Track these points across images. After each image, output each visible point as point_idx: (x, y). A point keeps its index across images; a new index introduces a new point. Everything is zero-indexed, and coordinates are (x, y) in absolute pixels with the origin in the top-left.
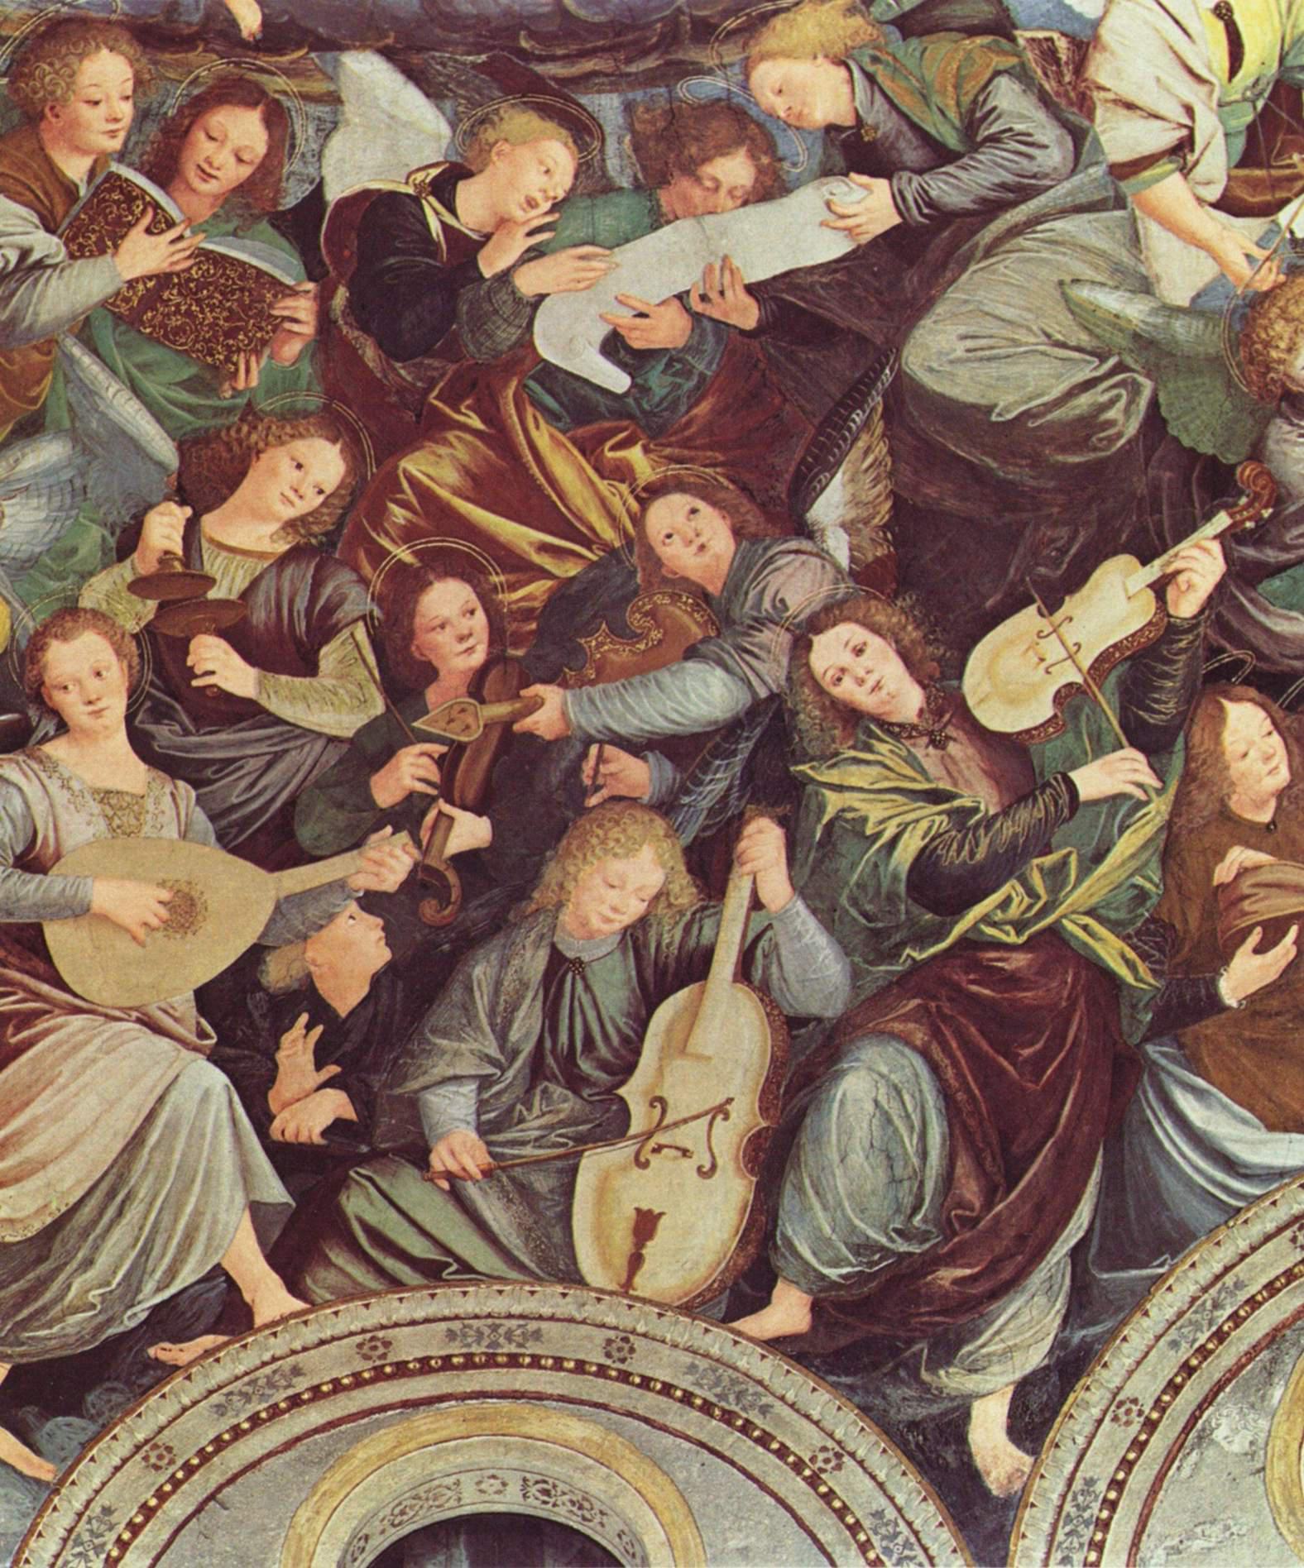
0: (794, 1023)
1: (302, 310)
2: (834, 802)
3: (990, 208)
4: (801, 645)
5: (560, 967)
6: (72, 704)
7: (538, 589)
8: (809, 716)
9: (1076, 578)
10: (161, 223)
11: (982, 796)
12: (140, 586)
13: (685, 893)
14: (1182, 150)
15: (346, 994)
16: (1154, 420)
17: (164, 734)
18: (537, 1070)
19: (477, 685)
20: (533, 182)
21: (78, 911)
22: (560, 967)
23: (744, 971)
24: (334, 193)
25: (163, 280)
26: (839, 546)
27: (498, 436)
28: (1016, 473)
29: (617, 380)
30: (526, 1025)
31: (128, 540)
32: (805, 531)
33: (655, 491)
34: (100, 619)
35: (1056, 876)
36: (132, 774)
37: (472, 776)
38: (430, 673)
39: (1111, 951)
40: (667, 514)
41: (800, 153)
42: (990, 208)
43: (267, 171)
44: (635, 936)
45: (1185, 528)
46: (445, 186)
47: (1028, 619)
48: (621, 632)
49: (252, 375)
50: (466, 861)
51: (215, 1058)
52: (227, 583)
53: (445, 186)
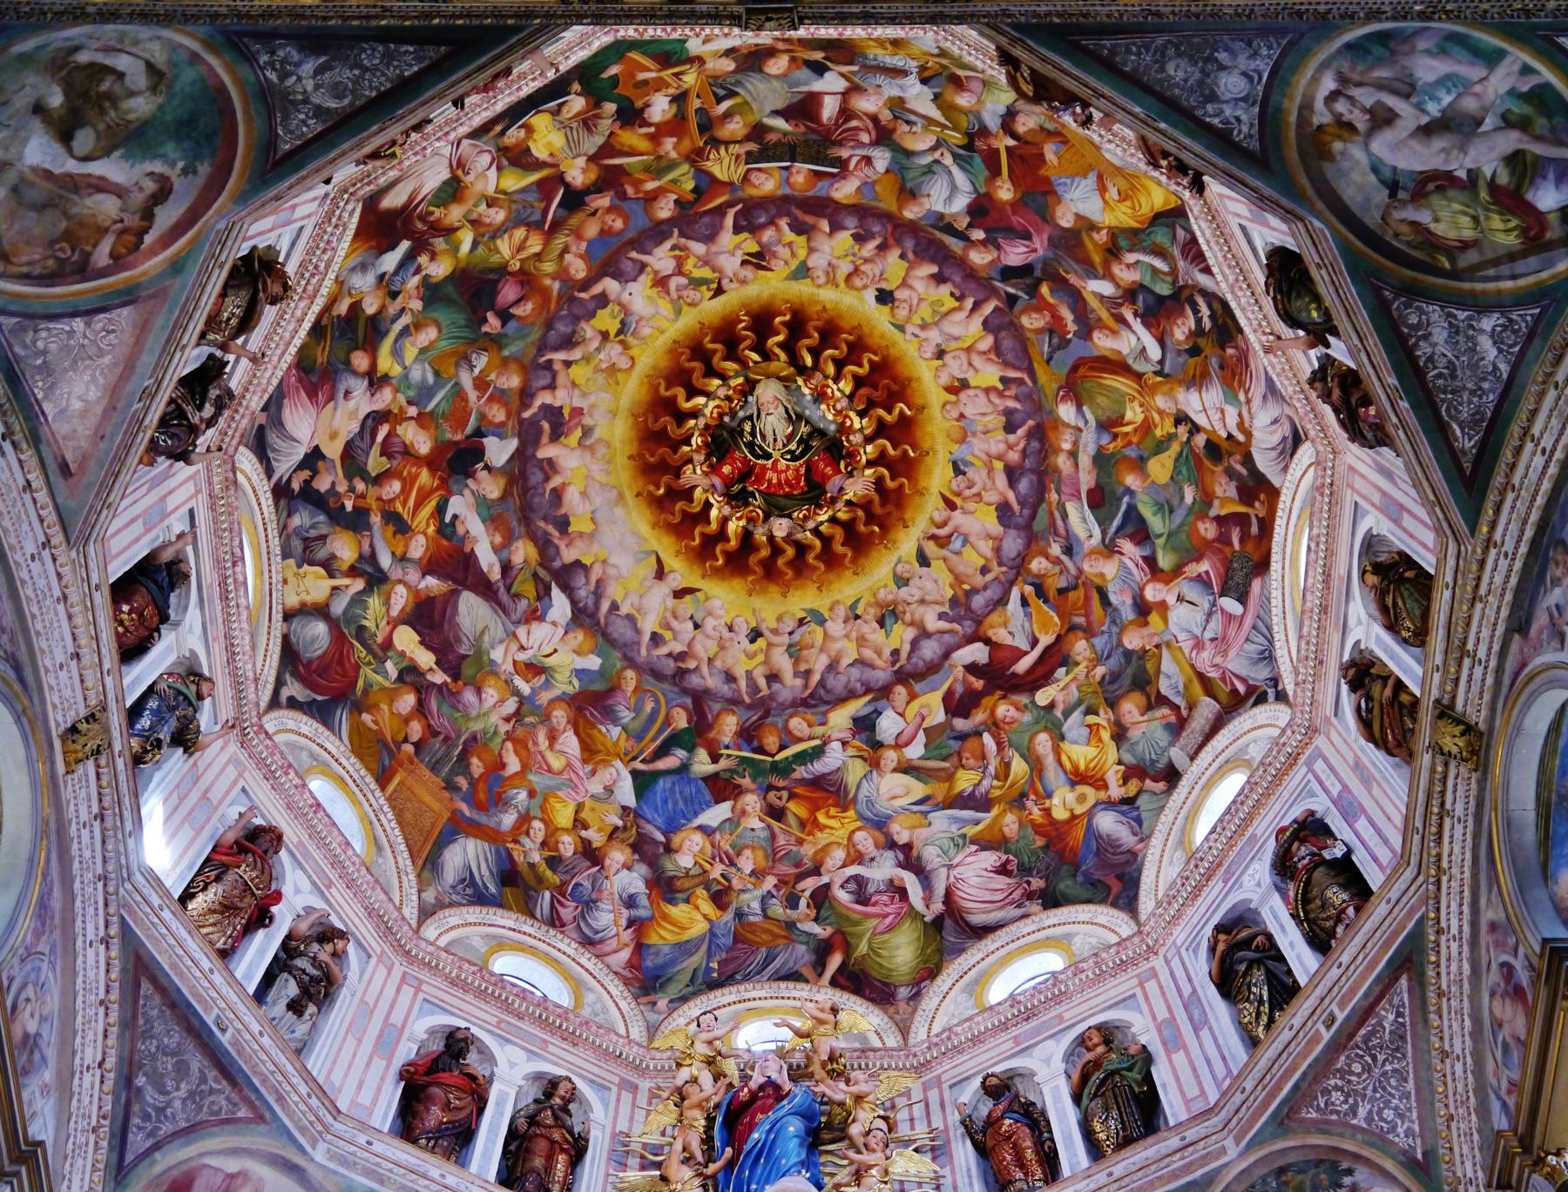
0: (327, 605)
1: (458, 437)
2: (370, 600)
3: (499, 604)
4: (400, 581)
5: (323, 538)
6: (378, 396)
7: (399, 508)
8: (385, 588)
9: (429, 647)
10: (479, 398)
11: (379, 639)
12: (401, 408)
13: (345, 567)
14: (522, 648)
15: (315, 485)
16: (464, 657)
17: (370, 422)
18: (305, 540)
19: (379, 499)
20: (488, 489)
21: (335, 409)
22: (323, 538)
23: (335, 588)
24: (485, 440)
25: (466, 401)
26: (422, 585)
27: (433, 491)
28: (446, 626)
29: (448, 519)
30: (313, 533)
31: (410, 403)
32: (423, 576)
33: (425, 533)
34: (394, 398)
35: (370, 663)
36: (361, 416)
37: (361, 503)
38: (381, 486)
39: (360, 684)
40: (421, 539)
41: (505, 554)
42: (499, 604)
43: (491, 423)
44: (333, 557)
45: (445, 671)
46: (487, 468)
47: (417, 638)
48: (395, 534)
49: (446, 427)
50: (343, 506)
51: (306, 455)
52: (400, 430)
53: (487, 468)
